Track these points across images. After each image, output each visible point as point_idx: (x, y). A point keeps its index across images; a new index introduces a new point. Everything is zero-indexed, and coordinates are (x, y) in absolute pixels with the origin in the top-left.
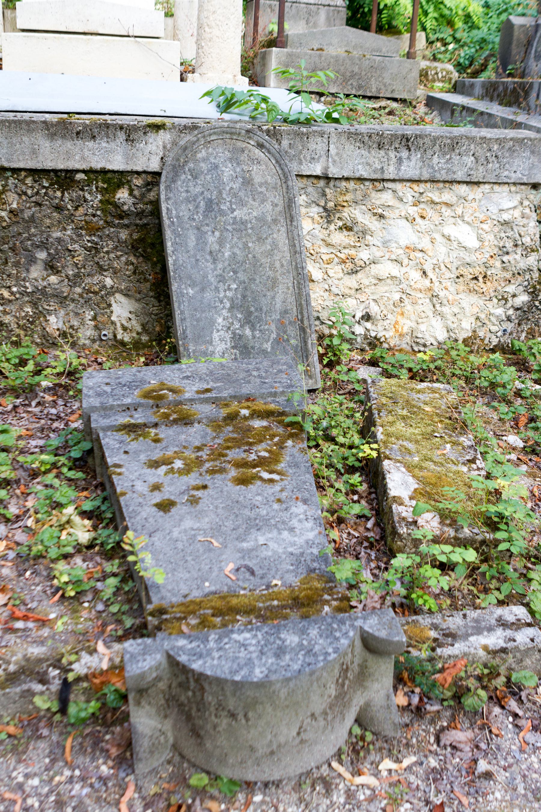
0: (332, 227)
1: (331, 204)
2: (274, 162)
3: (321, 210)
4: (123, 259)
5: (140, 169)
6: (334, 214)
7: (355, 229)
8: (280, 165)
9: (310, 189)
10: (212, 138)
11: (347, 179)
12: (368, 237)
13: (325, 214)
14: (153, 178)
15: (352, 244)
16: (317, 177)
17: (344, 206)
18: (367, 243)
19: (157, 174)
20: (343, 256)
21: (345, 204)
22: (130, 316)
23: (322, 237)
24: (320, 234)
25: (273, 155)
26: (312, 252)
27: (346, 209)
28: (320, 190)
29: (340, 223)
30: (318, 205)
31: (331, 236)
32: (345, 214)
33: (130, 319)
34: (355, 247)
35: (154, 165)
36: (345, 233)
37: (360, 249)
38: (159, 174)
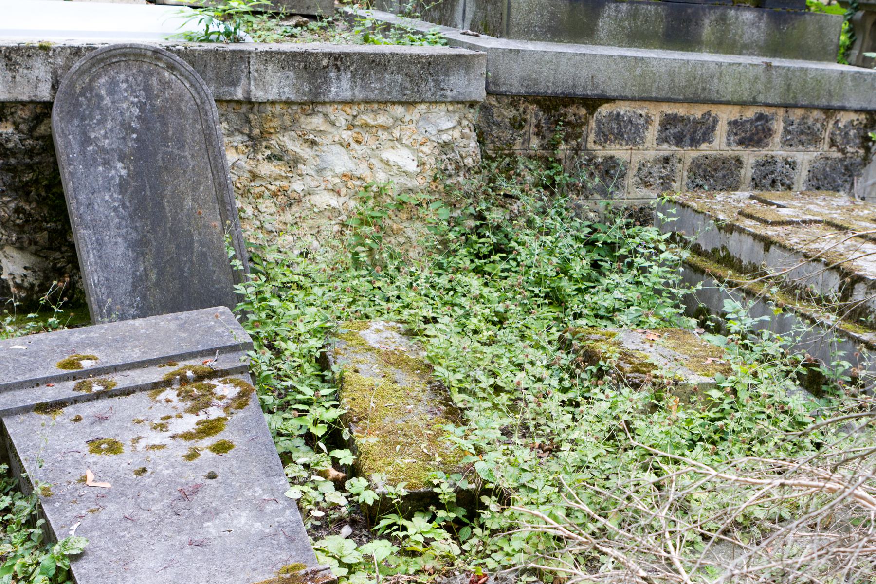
0: (260, 157)
1: (257, 131)
2: (188, 85)
3: (246, 138)
4: (12, 205)
5: (25, 98)
6: (260, 142)
8: (196, 89)
9: (231, 116)
10: (114, 60)
11: (273, 103)
12: (300, 166)
14: (43, 111)
15: (284, 174)
16: (238, 102)
17: (271, 133)
18: (299, 172)
19: (48, 105)
20: (273, 188)
21: (272, 131)
22: (25, 272)
23: (249, 168)
24: (246, 164)
25: (187, 78)
26: (238, 185)
27: (273, 137)
29: (268, 152)
30: (242, 133)
31: (260, 167)
32: (273, 142)
33: (25, 276)
34: (287, 177)
35: (44, 93)
36: (275, 162)
37: (292, 180)
38: (48, 105)
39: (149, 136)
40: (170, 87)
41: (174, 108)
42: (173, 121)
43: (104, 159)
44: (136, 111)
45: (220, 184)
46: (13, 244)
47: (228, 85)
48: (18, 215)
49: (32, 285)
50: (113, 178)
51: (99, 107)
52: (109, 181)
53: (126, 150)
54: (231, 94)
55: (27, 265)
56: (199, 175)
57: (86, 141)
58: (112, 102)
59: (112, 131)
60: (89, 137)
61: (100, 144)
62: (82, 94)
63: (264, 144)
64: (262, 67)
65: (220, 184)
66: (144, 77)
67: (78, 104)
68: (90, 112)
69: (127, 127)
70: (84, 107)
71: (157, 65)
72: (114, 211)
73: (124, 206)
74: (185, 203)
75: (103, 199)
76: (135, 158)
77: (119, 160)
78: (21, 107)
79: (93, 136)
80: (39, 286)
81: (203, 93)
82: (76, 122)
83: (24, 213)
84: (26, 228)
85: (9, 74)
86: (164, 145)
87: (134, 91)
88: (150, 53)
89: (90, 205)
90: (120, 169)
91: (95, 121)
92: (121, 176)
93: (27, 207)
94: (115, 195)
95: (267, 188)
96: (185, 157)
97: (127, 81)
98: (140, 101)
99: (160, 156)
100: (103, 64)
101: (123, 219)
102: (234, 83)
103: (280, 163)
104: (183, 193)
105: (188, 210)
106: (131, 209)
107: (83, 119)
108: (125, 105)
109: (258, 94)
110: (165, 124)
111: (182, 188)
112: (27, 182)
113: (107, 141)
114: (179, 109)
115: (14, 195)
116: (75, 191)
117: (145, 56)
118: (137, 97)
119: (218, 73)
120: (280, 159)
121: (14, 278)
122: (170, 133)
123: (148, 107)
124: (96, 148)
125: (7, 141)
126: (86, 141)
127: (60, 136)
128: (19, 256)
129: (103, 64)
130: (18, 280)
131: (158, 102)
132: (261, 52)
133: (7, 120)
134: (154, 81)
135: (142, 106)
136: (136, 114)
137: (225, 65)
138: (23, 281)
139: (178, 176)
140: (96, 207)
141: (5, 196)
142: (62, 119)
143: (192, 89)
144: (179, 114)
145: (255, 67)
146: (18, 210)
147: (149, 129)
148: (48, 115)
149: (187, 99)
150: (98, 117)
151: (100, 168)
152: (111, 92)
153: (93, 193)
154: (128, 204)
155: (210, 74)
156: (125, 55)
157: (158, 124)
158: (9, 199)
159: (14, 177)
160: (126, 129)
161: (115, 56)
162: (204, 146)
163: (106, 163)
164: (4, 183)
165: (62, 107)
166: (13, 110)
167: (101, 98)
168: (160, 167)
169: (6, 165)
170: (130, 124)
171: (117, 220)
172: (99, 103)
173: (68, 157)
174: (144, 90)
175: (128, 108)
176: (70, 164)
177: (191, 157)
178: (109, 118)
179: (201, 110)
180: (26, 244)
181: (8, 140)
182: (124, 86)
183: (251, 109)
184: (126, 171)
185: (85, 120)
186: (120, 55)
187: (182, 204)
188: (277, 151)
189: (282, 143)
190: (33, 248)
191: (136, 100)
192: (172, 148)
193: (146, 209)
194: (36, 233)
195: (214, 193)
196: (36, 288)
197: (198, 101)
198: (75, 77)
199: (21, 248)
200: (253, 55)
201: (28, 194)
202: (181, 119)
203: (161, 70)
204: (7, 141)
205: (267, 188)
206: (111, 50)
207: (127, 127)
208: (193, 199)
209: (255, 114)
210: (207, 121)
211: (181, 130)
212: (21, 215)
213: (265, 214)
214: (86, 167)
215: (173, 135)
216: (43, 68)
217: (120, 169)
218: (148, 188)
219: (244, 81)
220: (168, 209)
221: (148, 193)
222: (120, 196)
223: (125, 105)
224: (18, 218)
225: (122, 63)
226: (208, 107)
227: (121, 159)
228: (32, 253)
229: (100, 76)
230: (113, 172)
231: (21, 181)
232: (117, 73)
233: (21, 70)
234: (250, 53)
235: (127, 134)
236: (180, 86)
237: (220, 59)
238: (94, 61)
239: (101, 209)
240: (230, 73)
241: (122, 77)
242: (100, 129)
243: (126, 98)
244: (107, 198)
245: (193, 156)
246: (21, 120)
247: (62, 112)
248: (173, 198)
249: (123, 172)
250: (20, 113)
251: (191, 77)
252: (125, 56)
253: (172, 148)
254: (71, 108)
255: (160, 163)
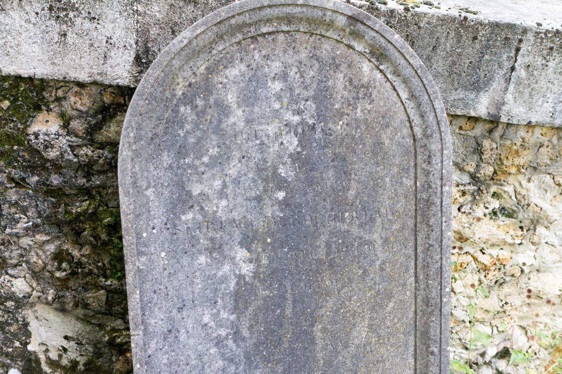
0: (480, 211)
1: (489, 170)
2: (404, 96)
3: (466, 179)
4: (51, 248)
5: (83, 77)
6: (488, 186)
7: (520, 216)
8: (419, 105)
10: (264, 30)
12: (540, 230)
13: (472, 188)
14: (114, 101)
15: (510, 240)
16: (476, 120)
18: (536, 239)
19: (126, 92)
20: (485, 260)
22: (65, 344)
25: (405, 81)
27: (511, 179)
28: (473, 141)
29: (495, 204)
32: (509, 189)
33: (65, 350)
35: (120, 71)
36: (502, 220)
38: (126, 92)
39: (310, 196)
40: (368, 95)
41: (369, 141)
42: (361, 168)
43: (212, 240)
44: (292, 143)
45: (427, 302)
46: (48, 303)
47: (465, 88)
48: (60, 264)
49: (75, 363)
50: (224, 279)
51: (218, 131)
52: (214, 284)
53: (260, 225)
54: (466, 106)
55: (69, 335)
56: (391, 279)
57: (182, 200)
58: (248, 122)
59: (236, 182)
60: (189, 194)
61: (209, 208)
62: (187, 99)
63: (493, 189)
64: (540, 61)
65: (427, 302)
66: (320, 71)
67: (175, 121)
68: (199, 140)
69: (269, 178)
70: (188, 127)
71: (349, 47)
72: (217, 344)
73: (237, 336)
74: (354, 334)
75: (198, 321)
76: (275, 241)
77: (241, 244)
78: (76, 89)
79: (196, 190)
80: (85, 365)
81: (431, 117)
82: (166, 159)
83: (69, 262)
84: (71, 284)
85: (55, 27)
86: (336, 218)
87: (294, 100)
88: (341, 21)
89: (171, 331)
90: (243, 261)
91: (206, 159)
92: (240, 277)
93: (76, 253)
94: (224, 315)
95: (475, 259)
96: (370, 243)
97: (284, 76)
98: (303, 123)
99: (324, 238)
100: (240, 36)
101: (231, 360)
102: (477, 87)
103: (508, 221)
104: (354, 315)
105: (358, 347)
106: (250, 343)
107: (181, 153)
108: (271, 129)
109: (516, 110)
110: (344, 173)
111: (354, 305)
112: (79, 215)
113: (224, 203)
114: (379, 144)
115: (55, 230)
116: (143, 309)
117: (330, 25)
118: (299, 112)
119: (454, 63)
120: (511, 215)
121: (47, 351)
122: (352, 193)
123: (318, 135)
124: (199, 217)
125: (46, 147)
126: (182, 200)
127: (127, 194)
128: (58, 320)
129: (240, 36)
130: (54, 355)
131: (339, 127)
132: (547, 31)
133: (49, 110)
134: (339, 81)
135: (305, 133)
136: (291, 149)
137: (471, 51)
138: (60, 356)
139: (350, 280)
140: (183, 336)
141: (39, 232)
142: (137, 154)
143: (410, 105)
144: (375, 154)
145: (527, 60)
146: (59, 256)
147: (311, 182)
148: (122, 108)
149: (396, 123)
150: (214, 151)
151: (202, 259)
152: (248, 99)
153: (180, 309)
154: (245, 333)
155: (440, 64)
156: (289, 19)
157: (331, 173)
158: (45, 238)
159: (55, 206)
160: (266, 180)
161: (269, 21)
162: (410, 223)
163: (216, 249)
164: (39, 213)
165: (139, 128)
166: (60, 93)
167: (224, 109)
168: (319, 261)
169: (44, 184)
170: (275, 169)
171: (221, 363)
172: (220, 121)
173: (139, 236)
174: (315, 98)
175: (278, 136)
176: (140, 253)
177: (384, 246)
178: (236, 154)
179: (419, 148)
180: (69, 306)
181: (48, 146)
182: (277, 86)
183: (490, 131)
184: (252, 266)
185: (186, 155)
186: (279, 19)
187: (348, 334)
188: (510, 203)
189: (524, 192)
190: (80, 312)
191: (296, 119)
192: (350, 224)
193: (279, 342)
194: (86, 290)
195: (411, 315)
196: (81, 367)
197: (418, 131)
198: (176, 63)
199: (63, 310)
200: (530, 36)
201: (78, 233)
202: (377, 164)
203: (356, 58)
204: (46, 147)
205: (475, 259)
206: (261, 8)
207: (269, 178)
208: (370, 326)
209: (493, 140)
210: (427, 173)
211: (374, 185)
212: (64, 265)
213: (460, 296)
214: (173, 254)
215: (356, 197)
216: (121, 22)
217: (242, 262)
218: (289, 303)
219: (497, 84)
220: (320, 343)
221: (289, 312)
222: (233, 317)
223: (271, 129)
224: (59, 269)
225: (281, 37)
226: (435, 147)
227: (246, 243)
228: (78, 318)
229: (229, 62)
230: (226, 268)
231: (67, 212)
232: (267, 57)
233: (78, 21)
234: (525, 31)
235: (265, 191)
236: (388, 96)
237: (466, 37)
238: (223, 28)
239: (192, 341)
240: (475, 67)
241: (276, 66)
242: (213, 176)
243: (276, 114)
244: (206, 319)
245: (386, 241)
246: (75, 113)
247: (138, 138)
248: (334, 322)
249: (247, 269)
250: (73, 99)
251: (415, 81)
252: (289, 22)
253: (350, 224)
254: (160, 130)
255: (322, 254)
